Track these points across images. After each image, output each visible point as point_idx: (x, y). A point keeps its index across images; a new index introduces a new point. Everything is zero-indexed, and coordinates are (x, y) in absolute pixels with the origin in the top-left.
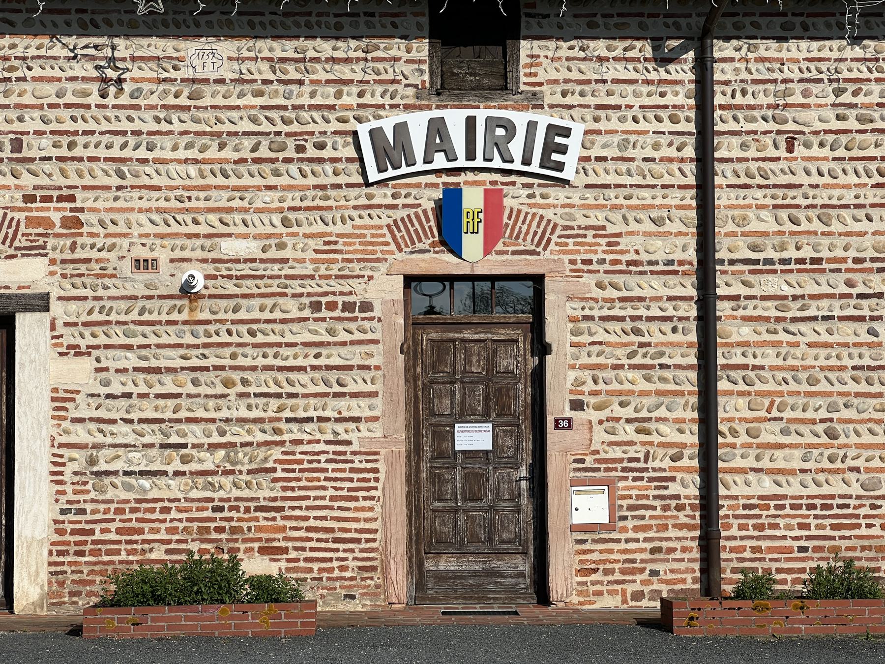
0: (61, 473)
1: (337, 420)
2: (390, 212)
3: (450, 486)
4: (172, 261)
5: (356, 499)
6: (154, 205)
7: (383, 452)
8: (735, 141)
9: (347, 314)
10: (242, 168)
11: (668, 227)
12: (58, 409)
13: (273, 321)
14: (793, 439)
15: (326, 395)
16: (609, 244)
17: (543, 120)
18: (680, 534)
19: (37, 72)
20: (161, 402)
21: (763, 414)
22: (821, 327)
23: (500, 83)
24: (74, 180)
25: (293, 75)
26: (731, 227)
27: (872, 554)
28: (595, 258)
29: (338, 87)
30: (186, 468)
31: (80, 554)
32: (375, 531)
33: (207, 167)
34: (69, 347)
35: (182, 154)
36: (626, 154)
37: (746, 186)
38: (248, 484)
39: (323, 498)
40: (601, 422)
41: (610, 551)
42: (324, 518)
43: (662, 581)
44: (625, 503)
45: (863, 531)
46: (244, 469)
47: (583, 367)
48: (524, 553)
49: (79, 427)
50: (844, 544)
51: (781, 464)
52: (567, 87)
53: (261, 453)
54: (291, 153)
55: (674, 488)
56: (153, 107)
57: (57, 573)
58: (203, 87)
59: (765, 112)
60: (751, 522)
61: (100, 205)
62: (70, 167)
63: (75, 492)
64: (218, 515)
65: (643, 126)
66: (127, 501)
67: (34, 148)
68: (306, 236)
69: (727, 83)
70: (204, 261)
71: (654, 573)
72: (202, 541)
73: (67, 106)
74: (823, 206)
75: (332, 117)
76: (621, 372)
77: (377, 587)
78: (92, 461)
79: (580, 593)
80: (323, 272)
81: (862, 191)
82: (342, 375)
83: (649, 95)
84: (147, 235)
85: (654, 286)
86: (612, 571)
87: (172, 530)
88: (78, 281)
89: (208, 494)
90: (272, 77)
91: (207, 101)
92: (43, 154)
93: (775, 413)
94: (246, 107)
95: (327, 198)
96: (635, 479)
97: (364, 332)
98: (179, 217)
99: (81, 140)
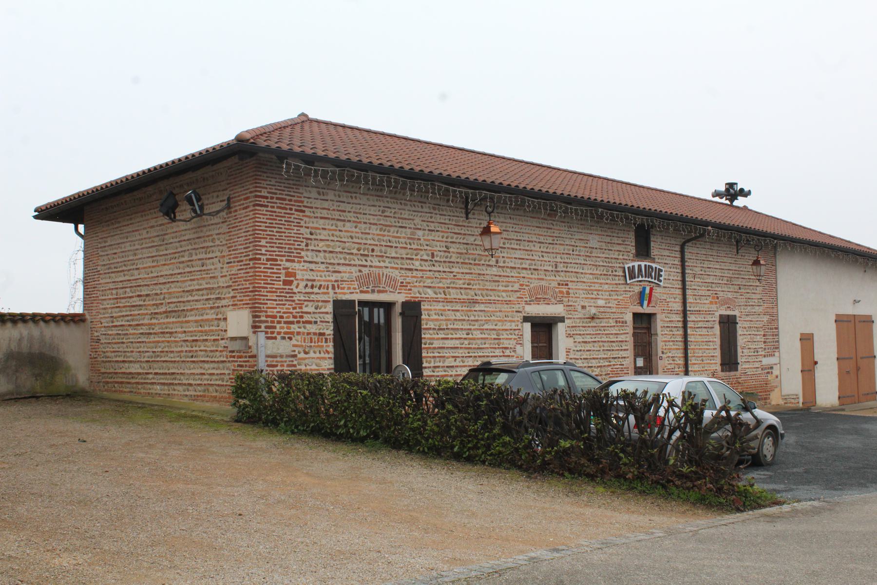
67: (561, 267)
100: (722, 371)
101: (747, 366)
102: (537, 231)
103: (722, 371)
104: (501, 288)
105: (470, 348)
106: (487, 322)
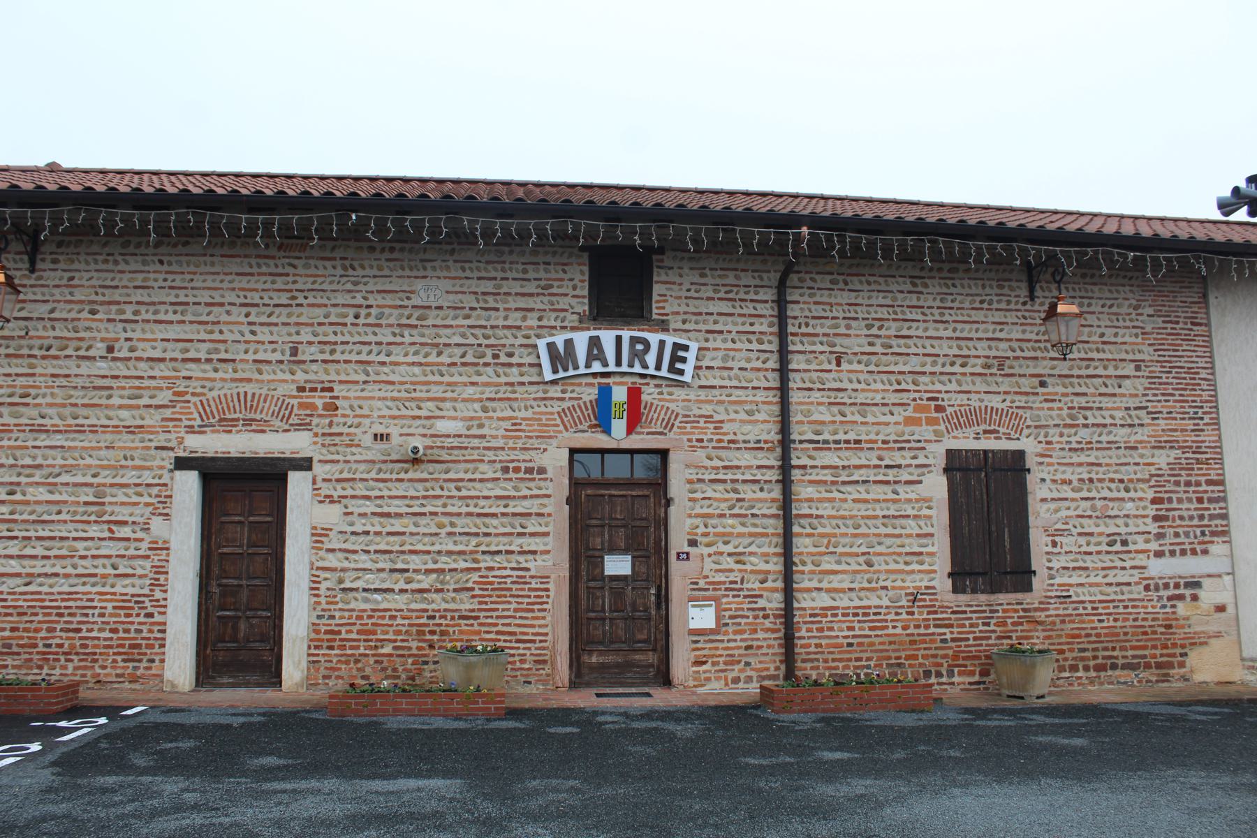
0: (317, 589)
1: (520, 553)
2: (559, 403)
3: (601, 602)
4: (401, 435)
5: (533, 611)
6: (389, 395)
7: (553, 576)
8: (800, 357)
9: (527, 476)
10: (453, 369)
11: (758, 416)
12: (317, 542)
13: (474, 480)
14: (843, 567)
15: (512, 534)
16: (715, 428)
17: (670, 340)
18: (766, 636)
19: (311, 300)
20: (392, 539)
21: (823, 549)
22: (861, 488)
24: (334, 377)
25: (492, 304)
26: (799, 417)
27: (896, 647)
28: (705, 438)
29: (524, 313)
30: (408, 587)
31: (331, 648)
32: (546, 634)
33: (428, 369)
34: (326, 497)
35: (410, 359)
36: (728, 365)
37: (810, 389)
38: (453, 600)
39: (508, 610)
40: (710, 555)
41: (717, 648)
42: (509, 625)
43: (753, 669)
44: (727, 614)
45: (891, 631)
46: (451, 587)
47: (697, 516)
48: (654, 650)
49: (330, 556)
50: (877, 640)
51: (835, 585)
52: (685, 317)
53: (465, 577)
54: (489, 359)
55: (761, 603)
56: (391, 326)
57: (314, 662)
58: (427, 311)
59: (821, 338)
60: (814, 626)
61: (351, 394)
62: (331, 367)
63: (328, 603)
64: (431, 622)
65: (738, 345)
66: (365, 611)
67: (307, 353)
68: (499, 419)
69: (795, 318)
70: (424, 436)
71: (747, 664)
72: (420, 641)
73: (331, 324)
74: (862, 404)
75: (519, 334)
76: (724, 520)
77: (548, 675)
78: (341, 581)
79: (695, 679)
80: (511, 444)
81: (886, 395)
82: (524, 521)
83: (743, 324)
84: (384, 417)
85: (746, 458)
86: (717, 663)
87: (398, 633)
88: (332, 449)
89: (424, 606)
90: (475, 305)
91: (429, 322)
92: (312, 358)
93: (831, 549)
94: (457, 326)
95: (515, 392)
96: (734, 596)
97: (540, 488)
98: (407, 404)
99: (339, 348)
100: (956, 590)
101: (1075, 580)
102: (243, 282)
103: (956, 590)
104: (116, 401)
105: (15, 521)
106: (68, 469)
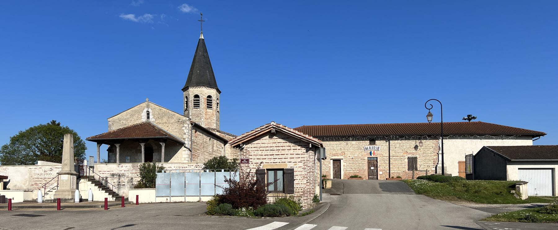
23: (374, 144)
